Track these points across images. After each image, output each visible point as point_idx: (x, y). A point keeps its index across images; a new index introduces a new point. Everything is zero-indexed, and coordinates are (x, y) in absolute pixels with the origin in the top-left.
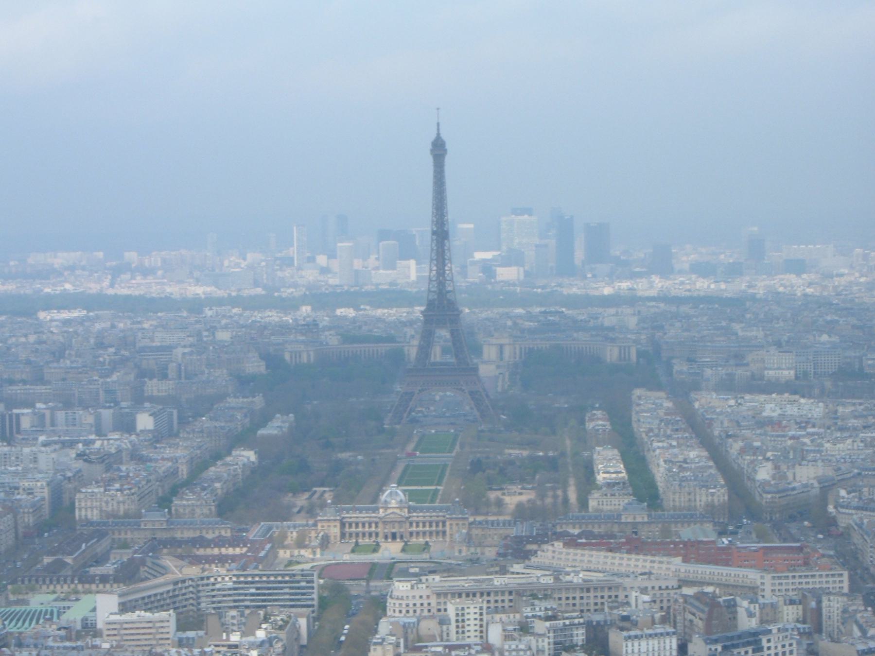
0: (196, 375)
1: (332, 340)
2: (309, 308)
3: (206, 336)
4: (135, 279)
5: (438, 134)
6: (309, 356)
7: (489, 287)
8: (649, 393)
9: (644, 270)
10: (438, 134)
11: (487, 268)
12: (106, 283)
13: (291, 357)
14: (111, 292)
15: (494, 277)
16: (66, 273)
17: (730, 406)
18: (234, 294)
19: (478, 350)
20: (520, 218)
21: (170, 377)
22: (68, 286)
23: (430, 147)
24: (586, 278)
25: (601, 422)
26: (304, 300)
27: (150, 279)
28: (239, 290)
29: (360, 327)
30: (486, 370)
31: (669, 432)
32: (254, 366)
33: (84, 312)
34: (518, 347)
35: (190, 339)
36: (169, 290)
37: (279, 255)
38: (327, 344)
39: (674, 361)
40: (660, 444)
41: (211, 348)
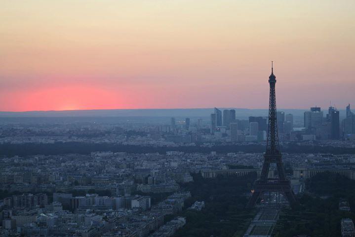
0: (161, 182)
2: (215, 152)
5: (272, 73)
6: (213, 175)
7: (299, 144)
10: (272, 73)
11: (299, 135)
12: (125, 139)
14: (125, 143)
15: (302, 139)
16: (106, 135)
18: (182, 145)
19: (291, 172)
21: (149, 183)
22: (106, 141)
23: (269, 79)
24: (344, 140)
25: (345, 207)
26: (213, 149)
27: (144, 138)
28: (185, 143)
29: (238, 162)
30: (293, 182)
32: (188, 179)
33: (112, 153)
34: (309, 171)
35: (159, 166)
36: (151, 143)
37: (204, 128)
38: (221, 169)
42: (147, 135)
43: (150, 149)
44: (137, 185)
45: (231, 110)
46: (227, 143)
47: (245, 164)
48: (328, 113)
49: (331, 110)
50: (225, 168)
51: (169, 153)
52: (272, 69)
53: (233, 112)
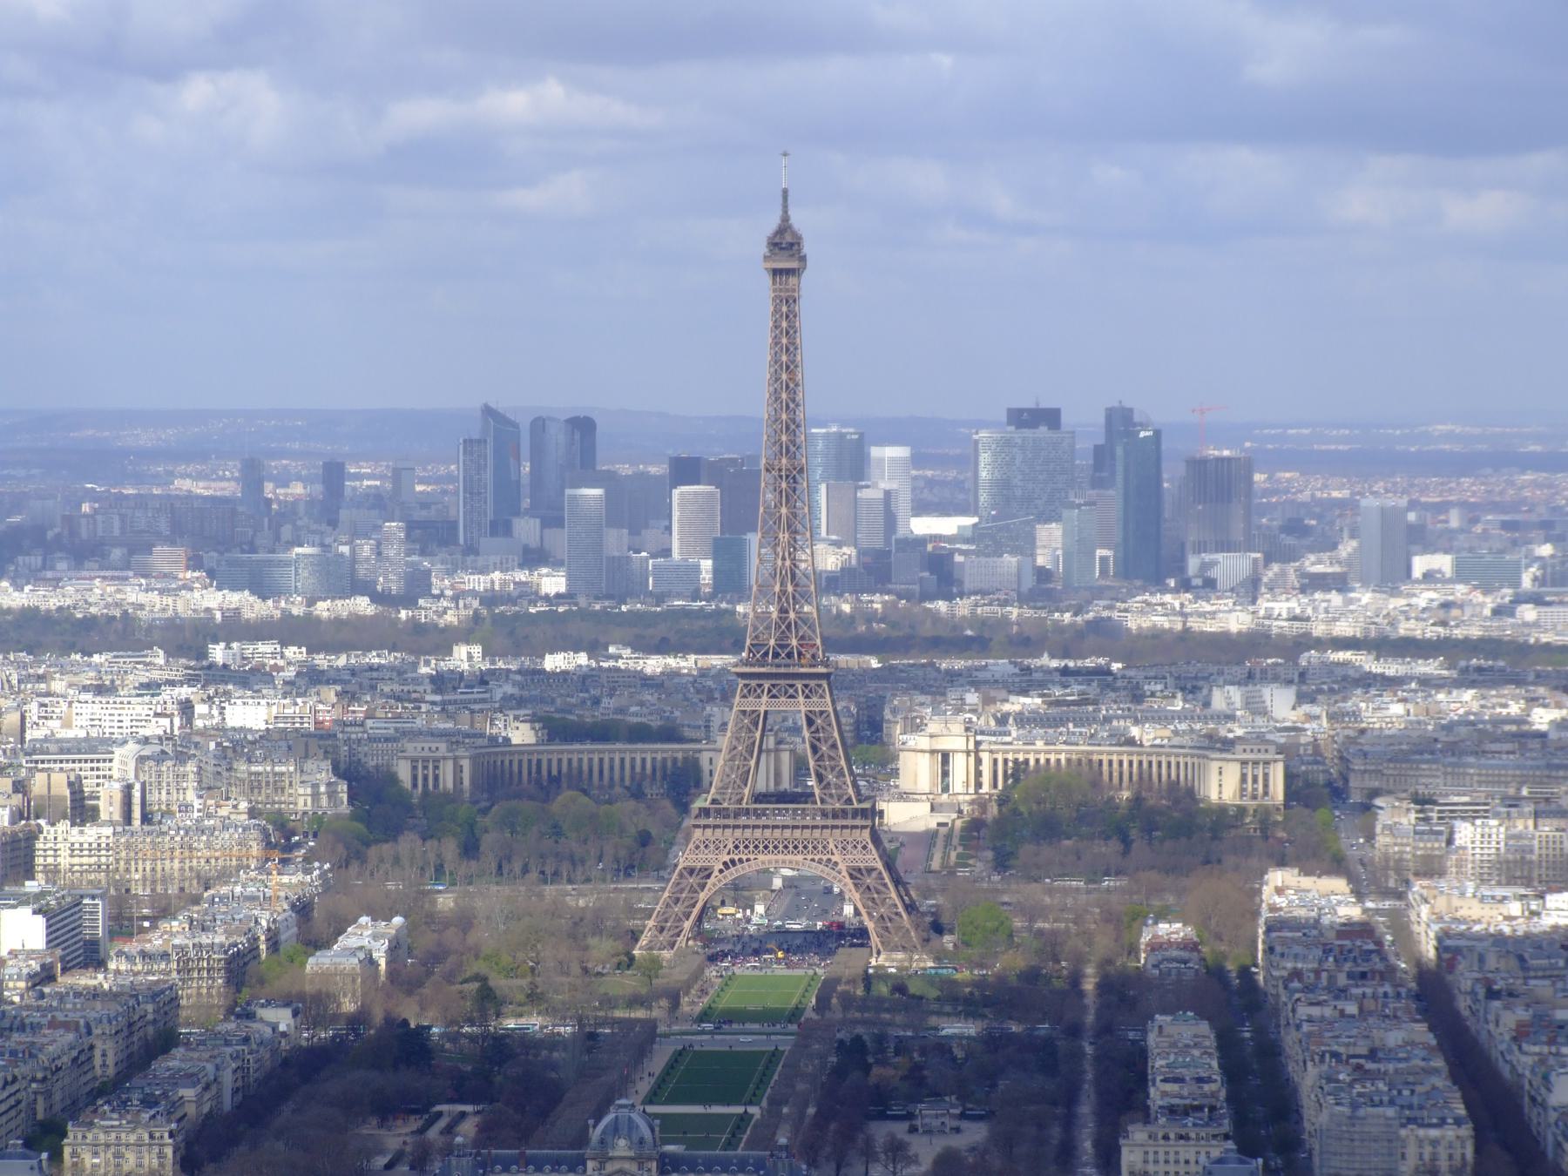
1: (521, 734)
2: (477, 650)
3: (202, 716)
4: (52, 568)
5: (785, 218)
6: (458, 769)
8: (1307, 882)
9: (1337, 569)
10: (785, 218)
13: (415, 778)
15: (961, 583)
17: (1509, 918)
18: (295, 611)
20: (1027, 433)
21: (104, 816)
23: (763, 249)
29: (596, 702)
31: (1342, 980)
35: (165, 722)
39: (1378, 802)
40: (1315, 1011)
41: (212, 745)
42: (104, 556)
43: (122, 633)
44: (33, 836)
45: (567, 421)
46: (547, 598)
47: (636, 716)
48: (1101, 441)
49: (1120, 421)
50: (521, 734)
51: (218, 653)
52: (785, 193)
53: (583, 427)
